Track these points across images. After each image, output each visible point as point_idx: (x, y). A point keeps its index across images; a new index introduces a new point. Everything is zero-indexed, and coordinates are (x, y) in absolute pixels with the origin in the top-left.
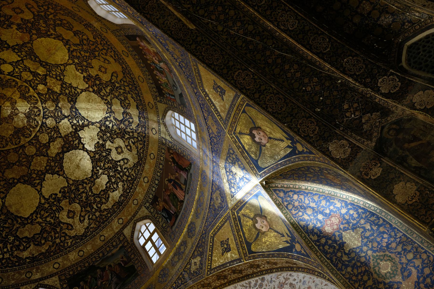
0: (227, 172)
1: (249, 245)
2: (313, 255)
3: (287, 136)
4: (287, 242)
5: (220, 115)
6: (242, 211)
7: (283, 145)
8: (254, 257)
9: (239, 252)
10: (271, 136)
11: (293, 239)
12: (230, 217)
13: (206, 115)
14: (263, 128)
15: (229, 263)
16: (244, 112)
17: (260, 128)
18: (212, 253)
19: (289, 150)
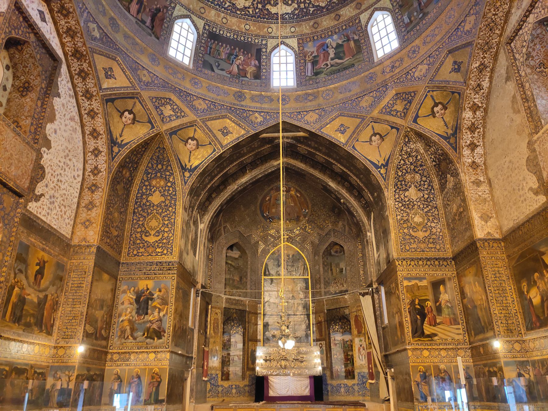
0: (167, 99)
1: (112, 100)
2: (116, 165)
3: (193, 167)
4: (117, 139)
5: (209, 120)
6: (138, 103)
7: (187, 161)
8: (103, 104)
9: (107, 89)
10: (192, 154)
11: (121, 146)
12: (135, 89)
13: (207, 102)
14: (198, 150)
15: (98, 75)
16: (210, 144)
17: (198, 148)
18: (104, 56)
19: (184, 165)
